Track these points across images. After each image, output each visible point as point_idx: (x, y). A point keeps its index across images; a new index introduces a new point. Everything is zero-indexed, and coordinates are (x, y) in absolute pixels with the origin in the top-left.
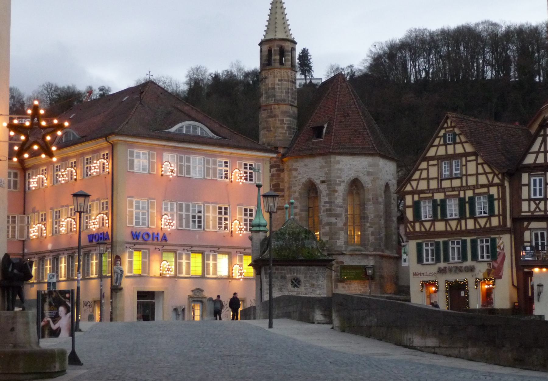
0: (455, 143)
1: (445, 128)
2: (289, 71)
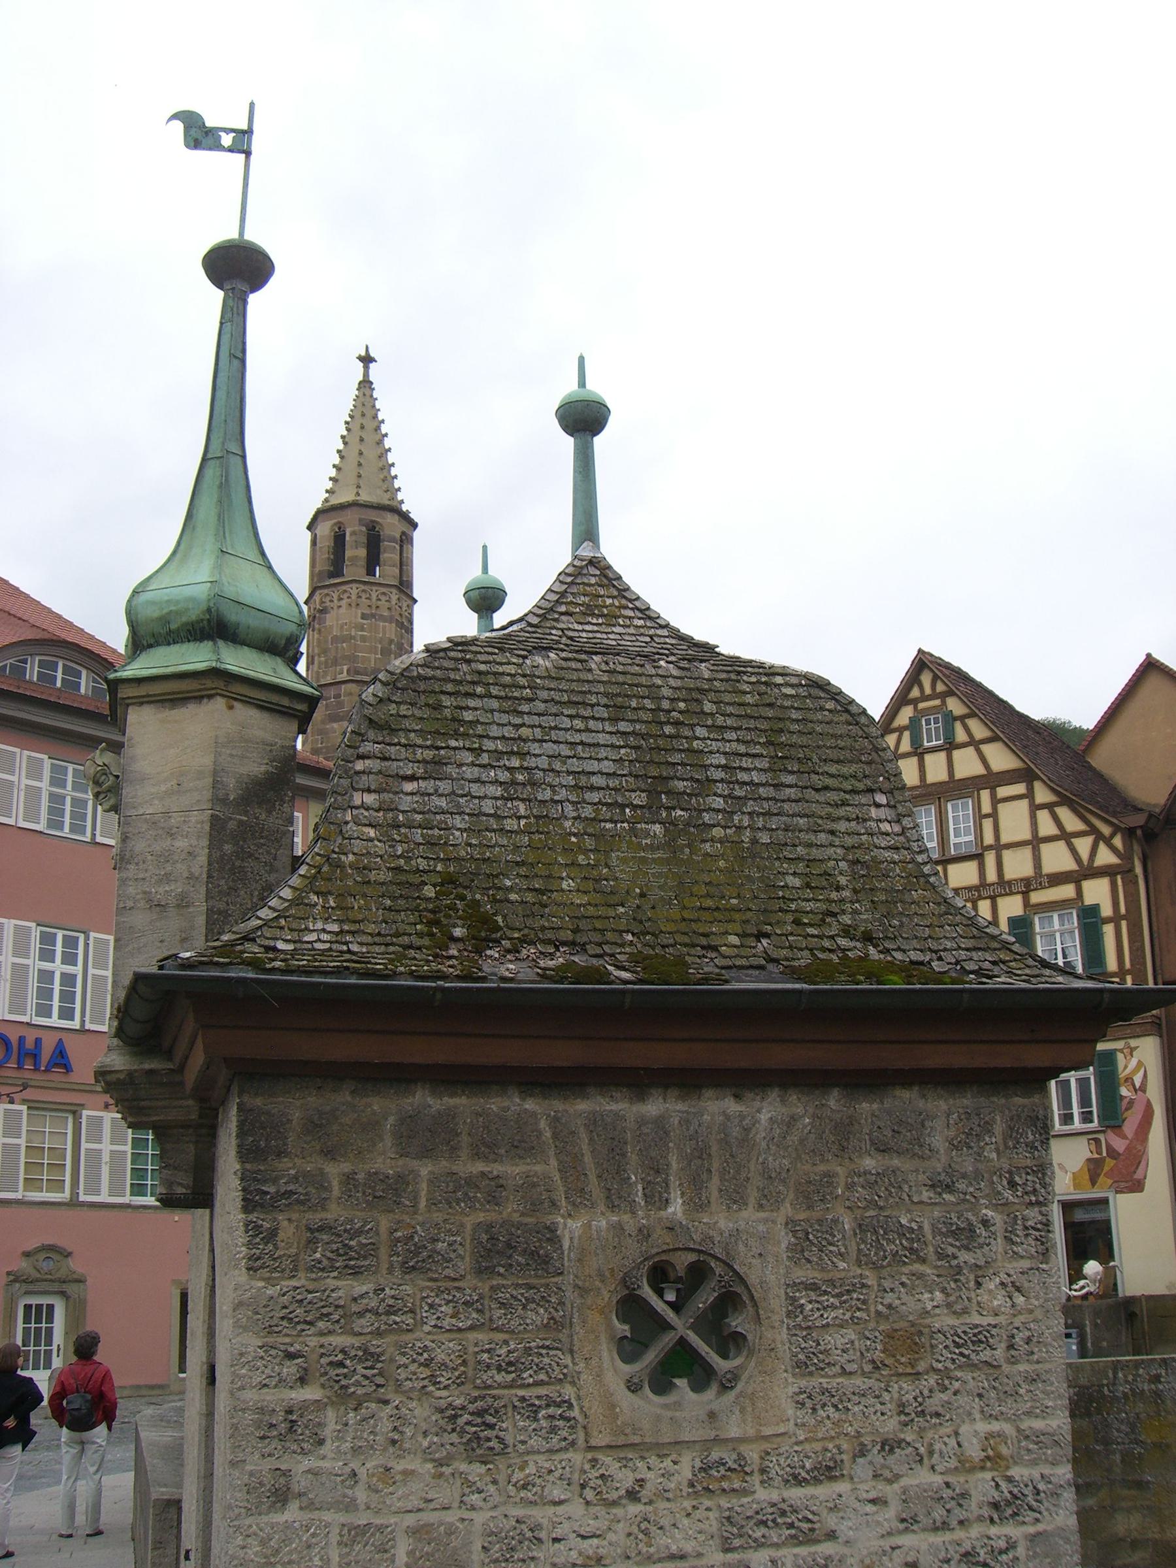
0: (950, 746)
1: (915, 702)
2: (394, 591)
